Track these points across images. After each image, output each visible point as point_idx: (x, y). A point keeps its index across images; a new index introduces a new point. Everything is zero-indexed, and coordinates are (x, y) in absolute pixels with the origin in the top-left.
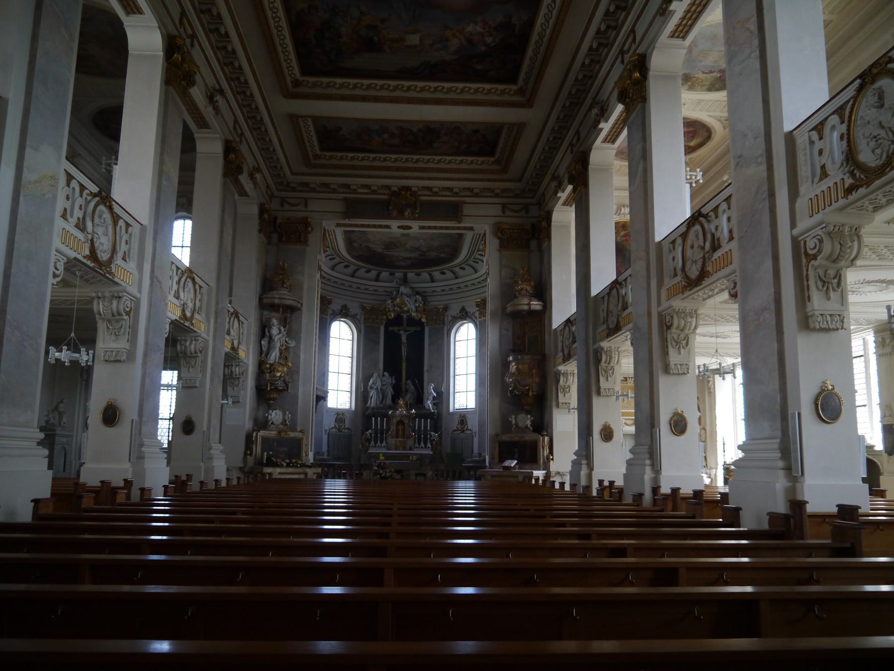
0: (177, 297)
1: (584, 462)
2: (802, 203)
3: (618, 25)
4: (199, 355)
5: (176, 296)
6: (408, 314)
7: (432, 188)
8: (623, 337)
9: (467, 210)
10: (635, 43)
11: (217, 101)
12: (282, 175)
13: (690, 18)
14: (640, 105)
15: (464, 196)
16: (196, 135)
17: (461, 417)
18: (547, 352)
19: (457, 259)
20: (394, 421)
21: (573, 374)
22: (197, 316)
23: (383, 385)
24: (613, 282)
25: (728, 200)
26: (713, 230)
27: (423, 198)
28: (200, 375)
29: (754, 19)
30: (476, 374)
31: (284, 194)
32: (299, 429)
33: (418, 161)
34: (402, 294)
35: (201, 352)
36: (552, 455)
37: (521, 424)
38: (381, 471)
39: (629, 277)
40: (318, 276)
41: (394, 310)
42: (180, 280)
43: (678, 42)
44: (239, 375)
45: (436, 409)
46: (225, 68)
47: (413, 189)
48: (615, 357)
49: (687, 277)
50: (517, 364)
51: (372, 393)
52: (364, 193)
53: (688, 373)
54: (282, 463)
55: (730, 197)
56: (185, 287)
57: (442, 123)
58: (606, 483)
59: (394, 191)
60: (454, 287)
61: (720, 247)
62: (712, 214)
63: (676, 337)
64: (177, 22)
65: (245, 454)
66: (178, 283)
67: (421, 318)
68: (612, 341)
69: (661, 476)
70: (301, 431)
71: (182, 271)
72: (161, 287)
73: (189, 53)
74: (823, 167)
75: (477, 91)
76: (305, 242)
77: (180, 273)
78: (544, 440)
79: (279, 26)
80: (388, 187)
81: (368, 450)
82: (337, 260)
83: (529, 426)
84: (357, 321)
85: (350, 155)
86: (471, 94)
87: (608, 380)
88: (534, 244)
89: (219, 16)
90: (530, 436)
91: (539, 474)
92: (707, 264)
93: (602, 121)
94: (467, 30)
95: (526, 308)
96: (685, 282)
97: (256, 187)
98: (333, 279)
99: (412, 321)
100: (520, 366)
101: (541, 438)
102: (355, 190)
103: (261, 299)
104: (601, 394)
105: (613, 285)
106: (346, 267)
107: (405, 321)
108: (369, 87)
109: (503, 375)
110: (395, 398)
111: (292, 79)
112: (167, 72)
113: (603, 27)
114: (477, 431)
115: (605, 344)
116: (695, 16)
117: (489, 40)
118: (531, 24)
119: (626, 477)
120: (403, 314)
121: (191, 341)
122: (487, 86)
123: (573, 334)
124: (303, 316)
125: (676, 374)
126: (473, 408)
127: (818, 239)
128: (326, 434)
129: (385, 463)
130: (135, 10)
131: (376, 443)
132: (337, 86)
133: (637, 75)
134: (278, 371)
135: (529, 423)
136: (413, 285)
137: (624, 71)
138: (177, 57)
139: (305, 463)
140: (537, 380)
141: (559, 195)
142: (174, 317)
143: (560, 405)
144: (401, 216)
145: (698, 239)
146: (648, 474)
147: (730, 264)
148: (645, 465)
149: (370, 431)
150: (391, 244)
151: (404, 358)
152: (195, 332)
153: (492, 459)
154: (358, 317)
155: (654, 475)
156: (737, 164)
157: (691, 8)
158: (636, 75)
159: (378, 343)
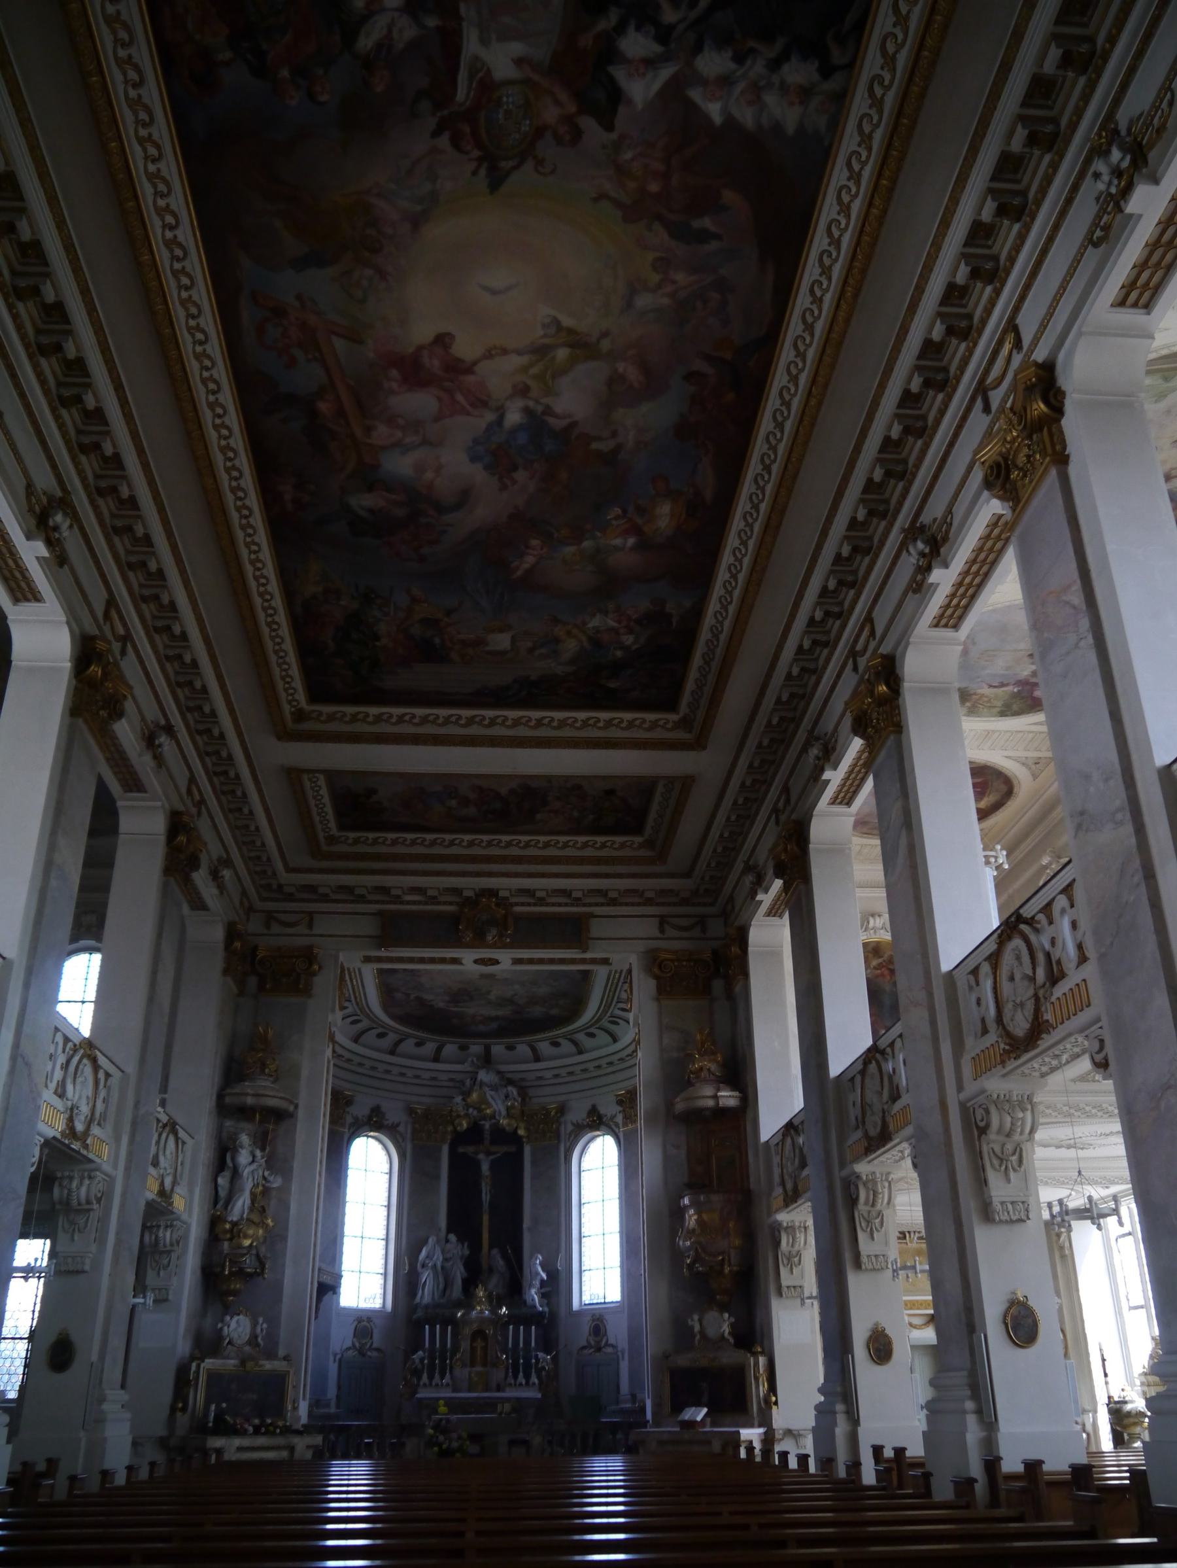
0: (61, 1093)
1: (840, 1407)
3: (842, 612)
4: (95, 1206)
5: (59, 1090)
6: (494, 1121)
7: (535, 890)
8: (895, 1153)
9: (597, 929)
11: (160, 746)
12: (270, 873)
13: (963, 596)
14: (892, 737)
15: (590, 905)
16: (119, 804)
17: (593, 1321)
18: (752, 1186)
19: (580, 1017)
20: (467, 1331)
21: (805, 1228)
22: (96, 1130)
23: (446, 1260)
24: (869, 1050)
25: (1068, 890)
26: (1047, 946)
27: (518, 909)
28: (94, 1248)
29: (1077, 586)
30: (621, 1232)
31: (271, 906)
32: (281, 1353)
33: (509, 844)
34: (482, 1084)
35: (99, 1200)
36: (776, 1395)
37: (711, 1332)
38: (441, 1438)
39: (899, 1040)
40: (329, 1052)
41: (467, 1115)
42: (68, 1062)
43: (948, 633)
44: (172, 1245)
45: (548, 1304)
46: (144, 606)
47: (502, 894)
48: (883, 1193)
49: (1008, 1034)
50: (699, 1213)
51: (426, 1276)
52: (414, 903)
53: (1029, 1219)
54: (246, 1426)
56: (79, 1073)
57: (549, 779)
58: (888, 1453)
59: (468, 898)
60: (577, 1069)
61: (1063, 975)
62: (1041, 917)
63: (997, 1149)
65: (173, 1409)
66: (65, 1067)
67: (517, 1128)
68: (875, 1162)
69: (1000, 1436)
70: (286, 1358)
71: (75, 1045)
72: (29, 1075)
73: (116, 664)
75: (609, 724)
76: (307, 992)
77: (70, 1049)
78: (756, 1364)
79: (239, 488)
80: (457, 891)
81: (415, 1392)
82: (365, 1024)
83: (726, 1334)
84: (398, 1136)
85: (391, 836)
86: (600, 728)
87: (873, 1238)
88: (718, 985)
89: (173, 607)
90: (730, 1357)
91: (751, 1434)
92: (1043, 1009)
93: (826, 767)
94: (590, 625)
95: (710, 1103)
96: (1005, 1044)
97: (222, 893)
98: (357, 1059)
99: (501, 1136)
100: (705, 1217)
101: (752, 1359)
102: (398, 897)
103: (220, 1097)
104: (863, 1267)
105: (870, 1055)
106: (381, 1036)
107: (487, 1136)
108: (425, 720)
109: (673, 1233)
110: (469, 1284)
111: (293, 709)
112: (74, 696)
113: (818, 615)
114: (626, 1346)
115: (862, 1168)
116: (991, 557)
117: (629, 640)
118: (698, 613)
119: (928, 1438)
120: (483, 1122)
121: (82, 1179)
122: (627, 716)
123: (801, 1150)
124: (299, 1126)
125: (1006, 1222)
126: (617, 1302)
128: (335, 1360)
129: (448, 1420)
130: (29, 596)
131: (431, 1378)
132: (370, 719)
133: (883, 688)
134: (246, 1237)
135: (726, 1329)
136: (503, 1068)
138: (95, 670)
139: (291, 1426)
140: (737, 1242)
141: (759, 897)
142: (50, 1133)
143: (785, 1290)
144: (479, 941)
145: (1021, 964)
146: (973, 1433)
147: (1087, 1007)
148: (964, 1412)
149: (420, 1353)
150: (463, 993)
151: (486, 1206)
152: (91, 1161)
153: (657, 1406)
154: (401, 1128)
155: (984, 1434)
156: (1079, 827)
157: (964, 579)
158: (880, 688)
159: (437, 1177)
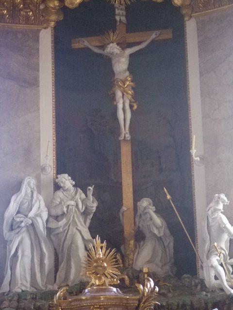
151: (125, 132)
159: (34, 83)
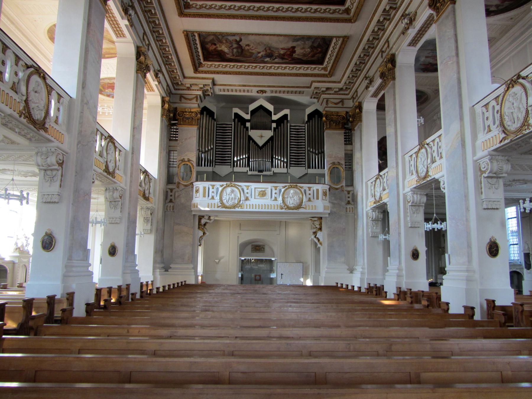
2: (479, 143)
10: (389, 48)
39: (386, 173)
55: (440, 136)
64: (142, 38)
74: (489, 126)
127: (486, 163)
130: (122, 35)
137: (383, 61)
